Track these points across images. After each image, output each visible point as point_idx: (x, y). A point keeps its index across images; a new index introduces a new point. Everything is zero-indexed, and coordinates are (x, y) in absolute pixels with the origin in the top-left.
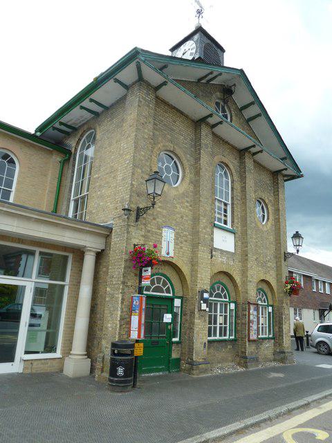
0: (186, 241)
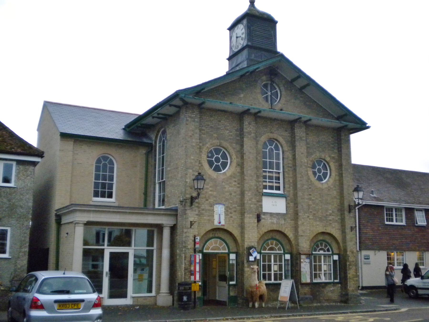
0: (235, 211)
